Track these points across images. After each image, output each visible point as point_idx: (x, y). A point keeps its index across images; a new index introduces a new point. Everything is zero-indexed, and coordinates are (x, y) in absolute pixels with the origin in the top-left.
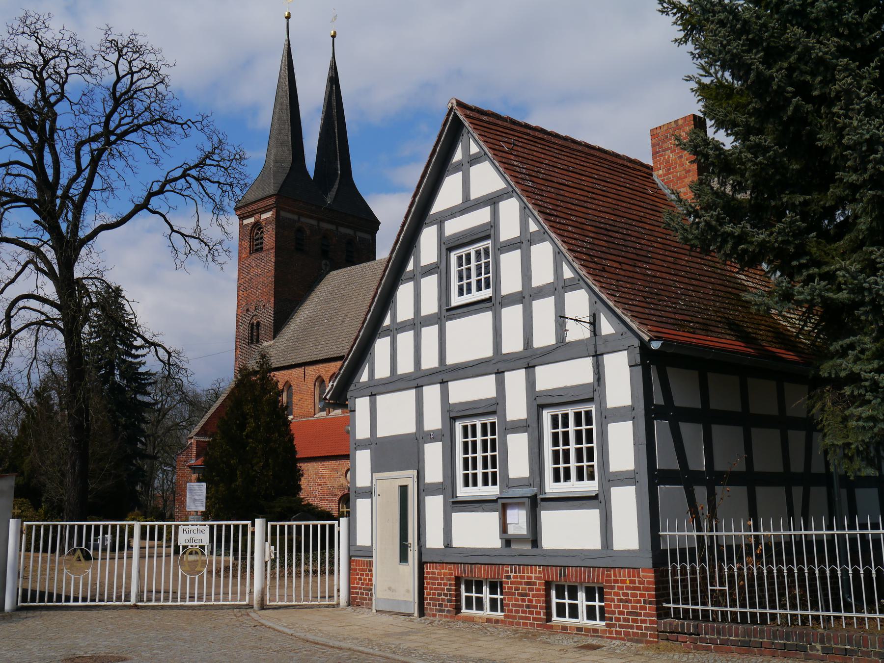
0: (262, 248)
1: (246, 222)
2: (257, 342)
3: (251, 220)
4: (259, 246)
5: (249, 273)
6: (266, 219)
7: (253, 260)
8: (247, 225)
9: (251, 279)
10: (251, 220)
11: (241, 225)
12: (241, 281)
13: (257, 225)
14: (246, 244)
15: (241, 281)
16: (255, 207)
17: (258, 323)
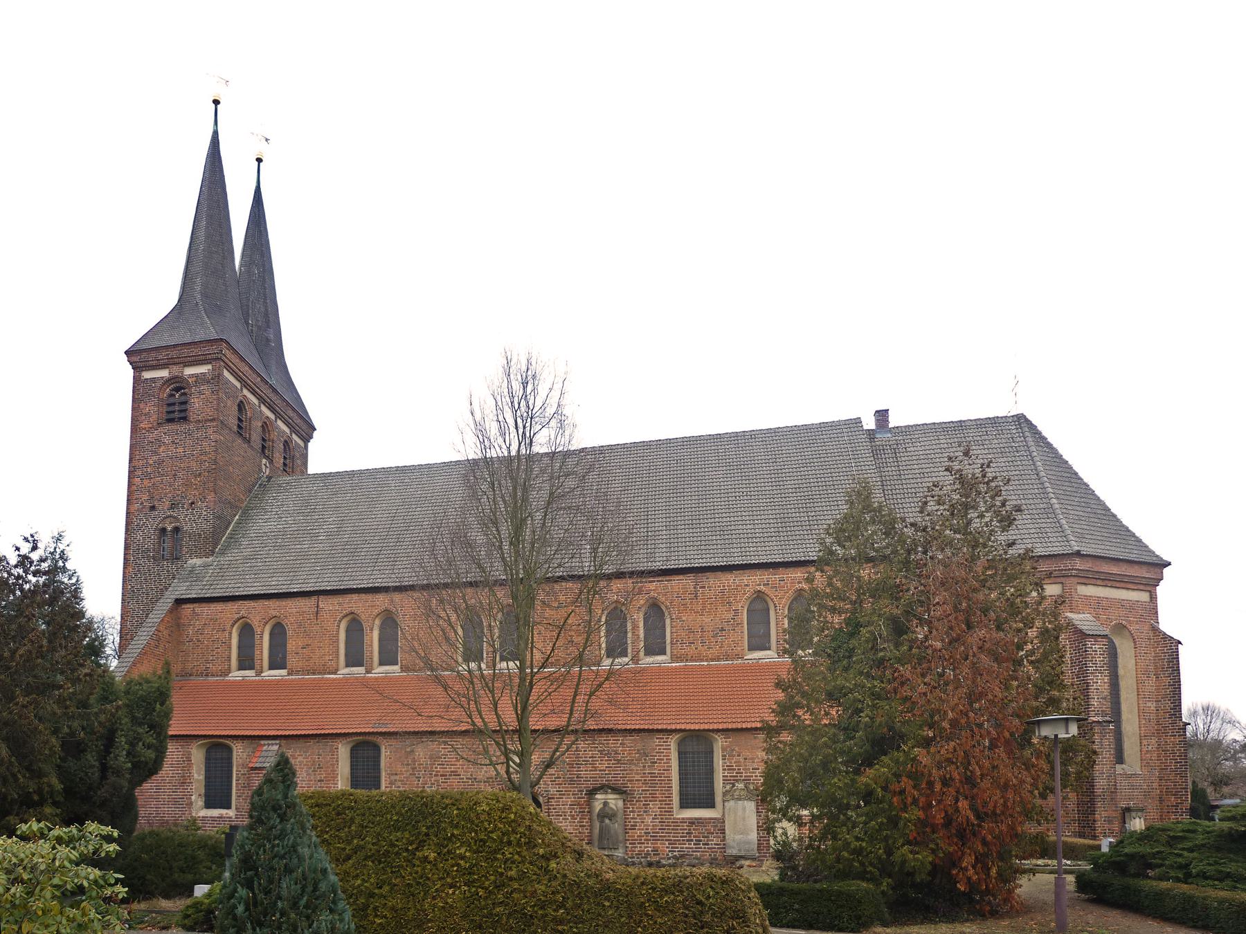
0: (185, 419)
1: (147, 375)
2: (176, 558)
3: (164, 373)
4: (176, 415)
5: (155, 453)
6: (196, 376)
7: (166, 434)
8: (153, 380)
9: (160, 463)
10: (164, 373)
11: (137, 380)
12: (135, 463)
13: (178, 385)
14: (150, 408)
15: (135, 463)
16: (174, 353)
17: (177, 529)
